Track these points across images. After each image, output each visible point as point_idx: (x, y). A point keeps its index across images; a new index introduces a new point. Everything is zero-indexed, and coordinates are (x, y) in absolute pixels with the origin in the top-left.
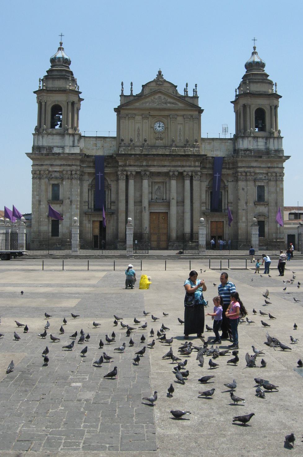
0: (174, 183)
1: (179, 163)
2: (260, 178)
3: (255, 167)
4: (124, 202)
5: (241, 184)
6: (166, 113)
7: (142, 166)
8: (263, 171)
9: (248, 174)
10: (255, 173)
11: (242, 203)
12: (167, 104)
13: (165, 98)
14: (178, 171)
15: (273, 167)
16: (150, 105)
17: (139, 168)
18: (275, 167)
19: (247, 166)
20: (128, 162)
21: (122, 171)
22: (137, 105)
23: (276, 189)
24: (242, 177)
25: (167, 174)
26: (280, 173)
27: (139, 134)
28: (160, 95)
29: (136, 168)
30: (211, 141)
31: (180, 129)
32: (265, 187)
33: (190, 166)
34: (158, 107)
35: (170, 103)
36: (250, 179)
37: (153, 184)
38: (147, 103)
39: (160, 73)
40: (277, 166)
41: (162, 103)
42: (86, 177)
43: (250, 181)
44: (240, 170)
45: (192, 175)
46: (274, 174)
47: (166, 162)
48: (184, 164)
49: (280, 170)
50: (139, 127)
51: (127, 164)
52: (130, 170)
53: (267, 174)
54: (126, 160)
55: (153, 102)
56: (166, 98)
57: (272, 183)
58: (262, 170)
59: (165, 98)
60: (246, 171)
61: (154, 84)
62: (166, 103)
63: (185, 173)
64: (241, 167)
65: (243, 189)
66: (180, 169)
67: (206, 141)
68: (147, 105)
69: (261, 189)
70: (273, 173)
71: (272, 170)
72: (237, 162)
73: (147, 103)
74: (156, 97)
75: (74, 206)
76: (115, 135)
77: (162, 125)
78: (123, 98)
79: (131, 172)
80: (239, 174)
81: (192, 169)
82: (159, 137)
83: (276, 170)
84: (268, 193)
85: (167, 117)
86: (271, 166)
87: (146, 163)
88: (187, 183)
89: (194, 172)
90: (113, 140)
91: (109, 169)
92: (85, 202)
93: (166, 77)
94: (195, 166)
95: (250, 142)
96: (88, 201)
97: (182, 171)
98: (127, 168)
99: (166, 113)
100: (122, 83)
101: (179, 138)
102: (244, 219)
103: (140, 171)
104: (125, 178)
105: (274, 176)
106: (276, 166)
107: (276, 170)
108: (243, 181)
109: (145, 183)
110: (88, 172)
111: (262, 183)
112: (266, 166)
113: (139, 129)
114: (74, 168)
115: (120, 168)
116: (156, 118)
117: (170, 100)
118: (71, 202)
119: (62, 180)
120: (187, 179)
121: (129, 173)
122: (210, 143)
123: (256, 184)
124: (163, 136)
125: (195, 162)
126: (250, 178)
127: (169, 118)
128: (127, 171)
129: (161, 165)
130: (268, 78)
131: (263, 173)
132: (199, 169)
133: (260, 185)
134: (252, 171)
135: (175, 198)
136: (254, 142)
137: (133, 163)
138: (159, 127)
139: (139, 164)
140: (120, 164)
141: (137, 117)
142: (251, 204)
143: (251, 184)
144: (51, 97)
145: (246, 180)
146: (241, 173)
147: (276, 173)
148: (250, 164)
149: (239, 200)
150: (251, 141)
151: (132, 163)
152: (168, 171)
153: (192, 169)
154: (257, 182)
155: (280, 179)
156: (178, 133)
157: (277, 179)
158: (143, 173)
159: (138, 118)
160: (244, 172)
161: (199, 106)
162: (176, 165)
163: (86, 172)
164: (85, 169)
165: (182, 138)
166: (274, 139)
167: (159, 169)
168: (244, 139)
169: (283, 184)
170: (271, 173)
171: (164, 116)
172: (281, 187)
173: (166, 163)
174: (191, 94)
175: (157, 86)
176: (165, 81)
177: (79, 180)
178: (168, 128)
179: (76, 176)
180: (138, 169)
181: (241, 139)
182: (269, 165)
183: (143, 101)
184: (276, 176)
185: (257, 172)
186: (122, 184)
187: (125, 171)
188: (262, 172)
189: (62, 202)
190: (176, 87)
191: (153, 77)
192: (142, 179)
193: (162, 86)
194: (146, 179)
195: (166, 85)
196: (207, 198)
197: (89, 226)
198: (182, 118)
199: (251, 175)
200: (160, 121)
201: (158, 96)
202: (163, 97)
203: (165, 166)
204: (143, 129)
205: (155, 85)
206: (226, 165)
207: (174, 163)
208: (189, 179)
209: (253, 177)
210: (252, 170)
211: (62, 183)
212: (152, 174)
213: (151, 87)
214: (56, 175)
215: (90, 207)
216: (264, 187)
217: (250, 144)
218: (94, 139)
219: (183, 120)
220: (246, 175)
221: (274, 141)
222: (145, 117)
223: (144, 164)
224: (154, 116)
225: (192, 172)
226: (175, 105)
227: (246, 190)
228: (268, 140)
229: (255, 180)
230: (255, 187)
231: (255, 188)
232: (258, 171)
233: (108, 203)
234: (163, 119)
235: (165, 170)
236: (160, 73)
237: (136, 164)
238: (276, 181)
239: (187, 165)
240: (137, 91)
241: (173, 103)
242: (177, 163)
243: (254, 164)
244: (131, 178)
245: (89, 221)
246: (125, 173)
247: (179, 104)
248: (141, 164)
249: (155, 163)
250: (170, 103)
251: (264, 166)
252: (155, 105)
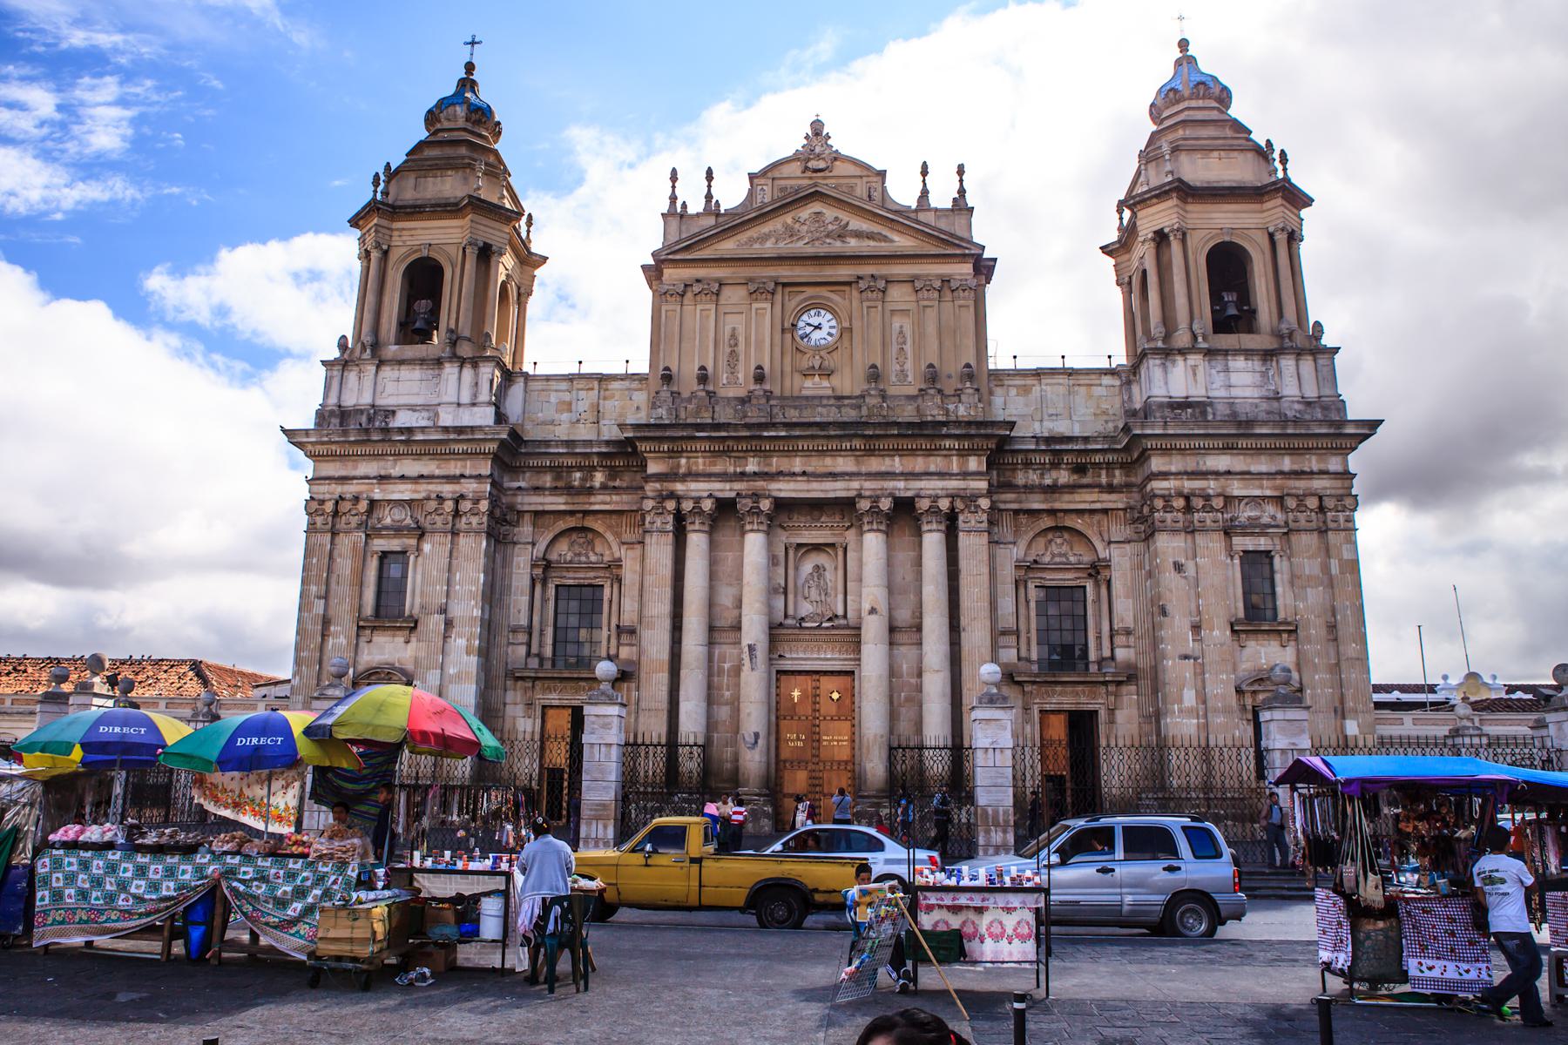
0: (873, 543)
1: (897, 464)
2: (1249, 518)
3: (1229, 473)
4: (666, 624)
5: (1169, 545)
6: (844, 272)
7: (742, 476)
8: (1262, 487)
9: (1198, 503)
10: (1229, 500)
11: (1177, 627)
12: (848, 239)
13: (836, 219)
14: (891, 495)
15: (1303, 473)
16: (781, 245)
17: (728, 486)
18: (1312, 473)
19: (1189, 470)
20: (683, 461)
21: (662, 498)
22: (728, 247)
23: (1326, 568)
24: (1169, 516)
25: (845, 506)
26: (1340, 498)
27: (733, 354)
28: (817, 207)
29: (718, 486)
30: (1029, 382)
31: (901, 332)
32: (1277, 560)
33: (941, 475)
34: (810, 250)
35: (858, 235)
36: (1208, 522)
37: (791, 553)
38: (769, 239)
39: (817, 128)
40: (1322, 467)
41: (828, 236)
42: (525, 530)
43: (1204, 530)
44: (1159, 485)
45: (952, 509)
46: (1312, 503)
47: (840, 460)
48: (919, 464)
49: (1338, 483)
50: (734, 329)
51: (682, 470)
52: (694, 494)
54: (674, 454)
55: (791, 233)
56: (844, 216)
57: (1307, 541)
58: (1257, 482)
59: (836, 219)
60: (1186, 491)
61: (795, 169)
62: (841, 236)
63: (924, 504)
64: (1164, 475)
65: (1178, 567)
66: (901, 484)
67: (1011, 383)
68: (769, 244)
69: (1257, 566)
70: (1305, 495)
71: (1301, 485)
72: (1144, 457)
73: (769, 239)
74: (805, 213)
75: (459, 643)
76: (646, 370)
77: (826, 319)
78: (674, 222)
79: (697, 500)
80: (1159, 503)
81: (954, 484)
82: (817, 367)
83: (1318, 484)
84: (1292, 584)
85: (847, 288)
86: (1296, 467)
87: (759, 464)
88: (933, 542)
89: (962, 498)
90: (635, 385)
91: (614, 497)
92: (515, 630)
93: (842, 142)
94: (965, 475)
95: (1195, 374)
96: (530, 626)
97: (909, 494)
98: (679, 487)
99: (844, 272)
100: (674, 172)
101: (898, 367)
103: (733, 495)
104: (670, 527)
105: (1312, 510)
106: (1315, 469)
107: (1318, 484)
108: (1174, 531)
109: (754, 544)
110: (533, 508)
111: (1262, 540)
112: (1273, 469)
113: (733, 336)
114: (469, 487)
115: (651, 488)
116: (802, 297)
117: (856, 224)
118: (449, 624)
119: (421, 536)
120: (934, 526)
121: (687, 506)
122: (1026, 390)
123: (1235, 548)
124: (830, 362)
125: (963, 456)
126: (1209, 517)
127: (855, 293)
128: (679, 499)
129: (821, 470)
131: (1264, 498)
132: (983, 485)
133: (1251, 548)
134: (1211, 492)
135: (883, 607)
136: (1214, 371)
137: (704, 464)
138: (818, 327)
139: (731, 469)
140: (653, 468)
141: (727, 292)
143: (1212, 544)
144: (405, 233)
145: (1191, 531)
146: (1166, 498)
147: (1320, 498)
148: (1201, 463)
149: (1164, 612)
150: (1201, 368)
151: (701, 467)
152: (852, 494)
153: (954, 484)
154: (1237, 534)
155: (1342, 520)
156: (895, 348)
157: (1325, 522)
158: (744, 505)
159: (734, 296)
160: (1180, 494)
161: (975, 240)
162: (883, 469)
163: (526, 508)
164: (519, 499)
165: (909, 366)
166: (1297, 360)
167: (815, 485)
168: (1168, 364)
169: (1355, 543)
170: (1297, 496)
172: (1346, 555)
173: (844, 464)
175: (809, 174)
176: (837, 157)
177: (484, 535)
178: (850, 330)
179: (475, 520)
180: (726, 490)
181: (1158, 362)
182: (1287, 464)
183: (753, 232)
184: (1322, 509)
185: (1236, 493)
186: (660, 551)
187: (672, 495)
188: (1257, 492)
189: (412, 626)
190: (882, 174)
191: (791, 142)
192: (743, 533)
193: (827, 174)
194: (758, 531)
195: (840, 168)
196: (1022, 611)
197: (529, 729)
198: (907, 288)
199: (1212, 507)
201: (809, 211)
202: (830, 213)
203: (833, 476)
204: (747, 339)
205: (799, 174)
206: (1099, 476)
207: (875, 464)
208: (943, 527)
209: (1220, 515)
210: (1212, 486)
211: (419, 549)
212: (784, 506)
213: (783, 183)
214: (397, 517)
215: (534, 650)
216: (1272, 558)
217: (1196, 381)
218: (564, 385)
219: (913, 298)
221: (1297, 366)
222: (758, 291)
223: (752, 466)
225: (953, 497)
226: (880, 240)
227: (1190, 569)
228: (1274, 364)
229: (1228, 532)
230: (1232, 557)
231: (1229, 561)
232: (1236, 488)
233: (609, 636)
234: (832, 296)
235: (836, 489)
236: (817, 128)
237: (718, 469)
238: (1323, 531)
239: (932, 468)
240: (731, 194)
241: (870, 236)
242: (888, 461)
243: (1221, 462)
244: (697, 527)
245: (529, 705)
246: (671, 505)
247: (896, 237)
248: (738, 470)
249: (797, 464)
250: (858, 235)
251: (1264, 468)
252: (801, 244)
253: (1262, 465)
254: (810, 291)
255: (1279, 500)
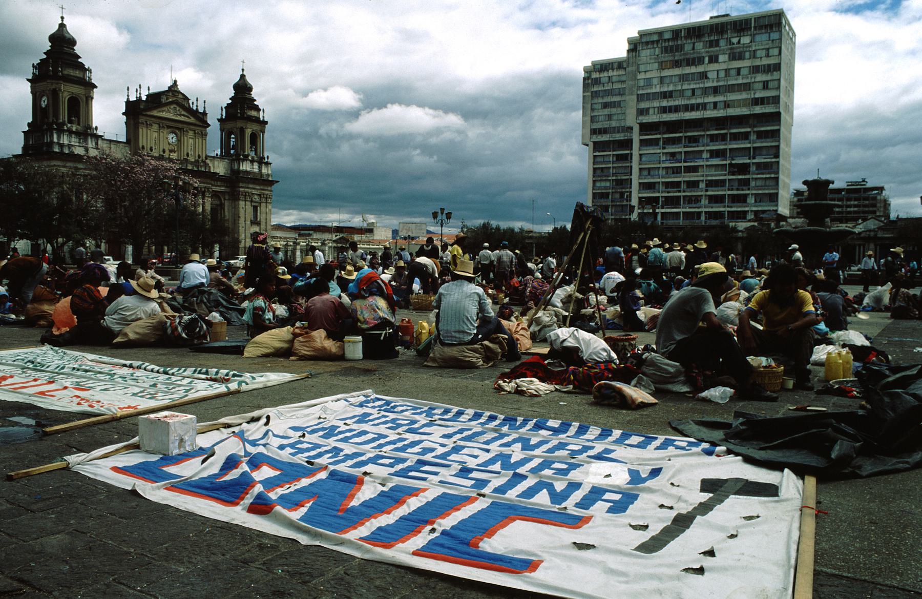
5: (242, 203)
6: (180, 126)
35: (184, 115)
53: (260, 195)
57: (263, 205)
62: (180, 115)
64: (242, 187)
77: (174, 135)
102: (243, 235)
130: (255, 103)
142: (248, 222)
143: (248, 203)
171: (179, 129)
174: (201, 110)
182: (262, 187)
195: (180, 96)
200: (173, 132)
202: (178, 108)
220: (246, 195)
224: (168, 127)
225: (205, 188)
232: (254, 192)
250: (184, 115)
253: (258, 187)
254: (172, 129)
255: (260, 195)
